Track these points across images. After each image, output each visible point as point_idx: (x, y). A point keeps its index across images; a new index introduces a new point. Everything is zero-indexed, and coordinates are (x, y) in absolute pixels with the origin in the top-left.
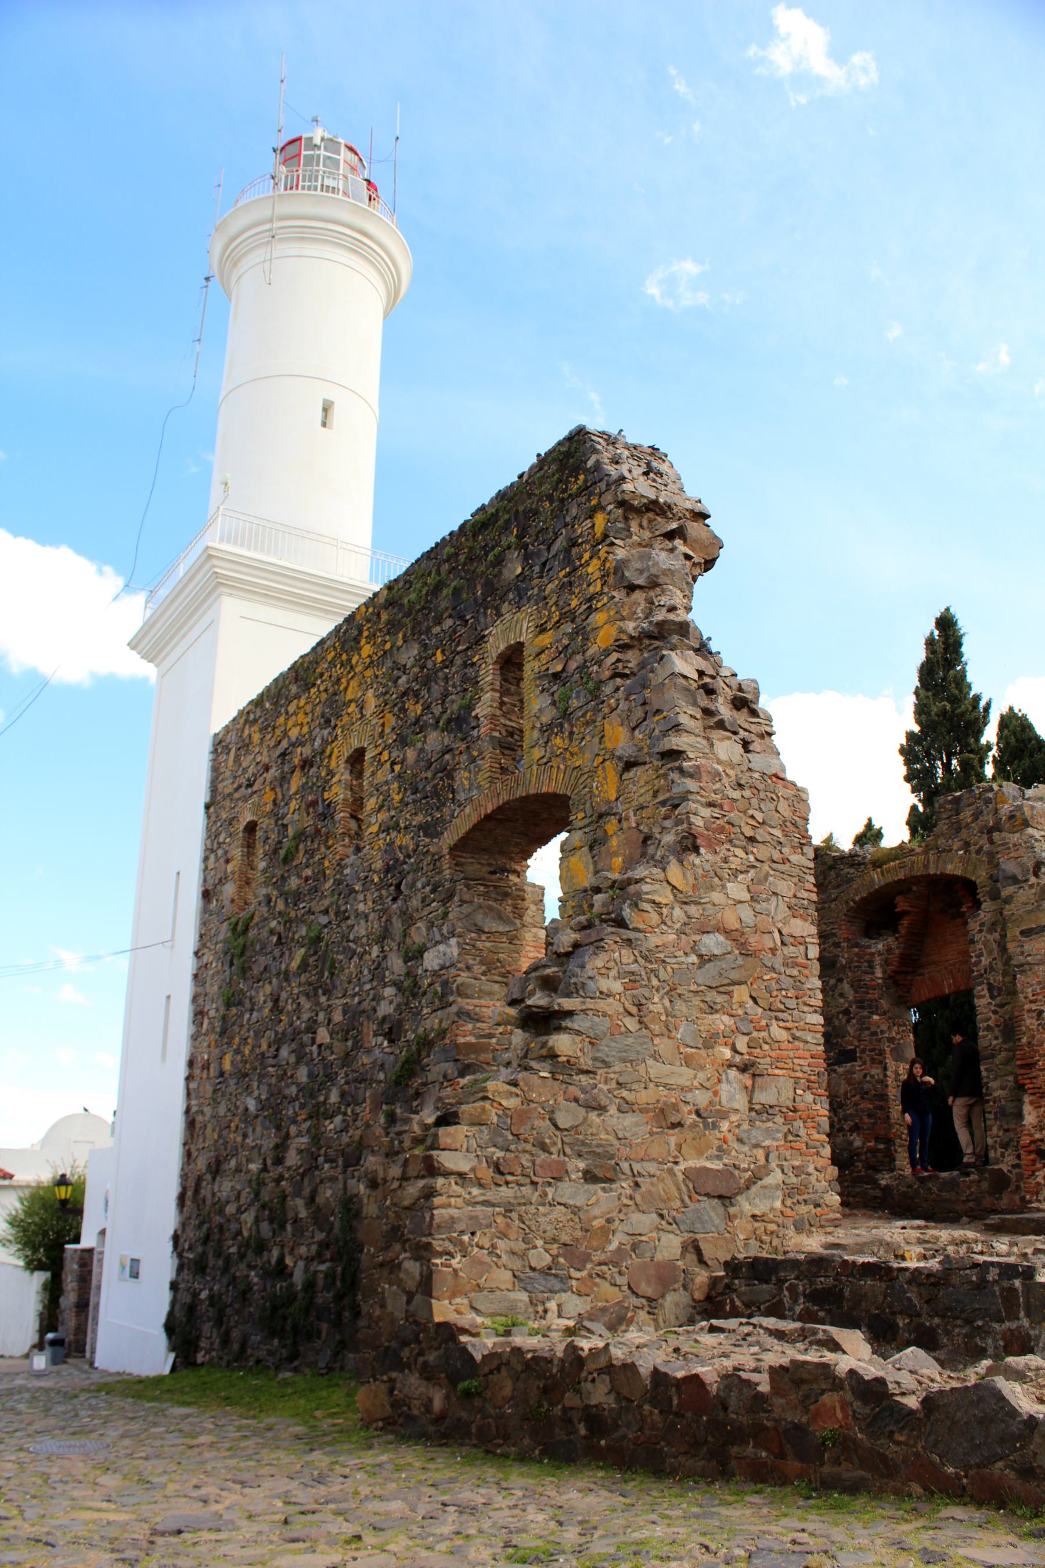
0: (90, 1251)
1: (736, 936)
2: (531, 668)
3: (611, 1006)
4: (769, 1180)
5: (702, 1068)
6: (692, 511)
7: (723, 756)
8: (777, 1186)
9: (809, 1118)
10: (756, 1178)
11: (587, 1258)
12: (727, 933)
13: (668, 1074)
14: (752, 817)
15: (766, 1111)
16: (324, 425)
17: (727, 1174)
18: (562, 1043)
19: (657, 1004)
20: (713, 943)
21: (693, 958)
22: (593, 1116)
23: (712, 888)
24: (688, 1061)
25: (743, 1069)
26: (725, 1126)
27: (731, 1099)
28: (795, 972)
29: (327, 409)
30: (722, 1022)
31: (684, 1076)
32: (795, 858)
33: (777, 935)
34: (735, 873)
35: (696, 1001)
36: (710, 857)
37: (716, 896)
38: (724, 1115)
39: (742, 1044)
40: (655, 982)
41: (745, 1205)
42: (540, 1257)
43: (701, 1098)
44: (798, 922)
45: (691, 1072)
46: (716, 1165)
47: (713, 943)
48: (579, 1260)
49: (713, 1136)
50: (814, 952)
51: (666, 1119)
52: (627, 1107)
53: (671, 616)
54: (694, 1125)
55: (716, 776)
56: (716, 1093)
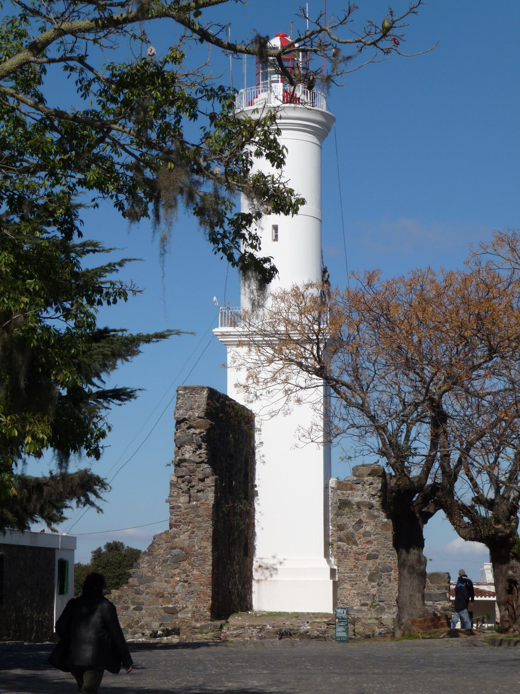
3: (145, 571)
4: (186, 609)
5: (170, 583)
6: (198, 417)
9: (205, 594)
10: (183, 608)
11: (133, 627)
13: (158, 585)
15: (192, 593)
16: (276, 239)
17: (174, 608)
18: (130, 580)
19: (158, 569)
20: (175, 552)
21: (169, 556)
22: (138, 596)
23: (176, 538)
24: (166, 581)
25: (185, 582)
26: (177, 596)
27: (179, 590)
29: (275, 228)
30: (177, 571)
31: (165, 585)
32: (205, 525)
33: (197, 547)
34: (184, 533)
35: (169, 567)
36: (176, 529)
37: (176, 540)
38: (177, 594)
39: (183, 576)
40: (157, 563)
41: (179, 615)
43: (170, 590)
44: (205, 543)
45: (166, 584)
47: (175, 552)
48: (132, 627)
49: (173, 599)
50: (209, 549)
51: (160, 595)
52: (147, 594)
53: (182, 458)
54: (167, 597)
55: (180, 507)
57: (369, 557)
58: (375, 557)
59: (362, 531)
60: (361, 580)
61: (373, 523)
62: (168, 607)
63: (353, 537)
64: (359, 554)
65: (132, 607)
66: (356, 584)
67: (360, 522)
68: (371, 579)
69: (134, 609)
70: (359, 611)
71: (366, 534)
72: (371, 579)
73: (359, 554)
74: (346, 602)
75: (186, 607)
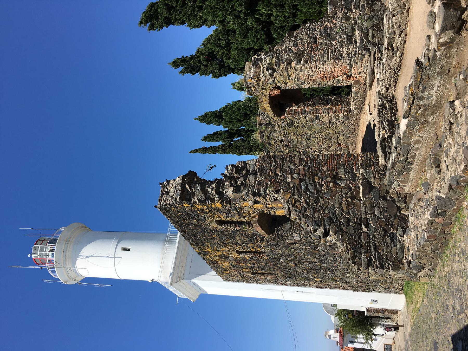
0: (367, 309)
1: (301, 180)
2: (223, 219)
7: (253, 181)
8: (366, 171)
12: (301, 182)
14: (269, 173)
16: (129, 250)
26: (351, 185)
28: (309, 162)
29: (125, 249)
33: (299, 167)
37: (291, 185)
39: (329, 179)
42: (388, 240)
46: (361, 188)
55: (259, 184)
56: (343, 187)
57: (316, 42)
58: (315, 38)
59: (293, 48)
60: (335, 46)
61: (287, 42)
62: (363, 192)
63: (297, 53)
64: (312, 49)
65: (364, 229)
66: (337, 48)
67: (285, 50)
68: (335, 39)
69: (367, 226)
70: (362, 41)
71: (296, 45)
72: (335, 39)
73: (312, 49)
74: (353, 53)
75: (362, 174)
